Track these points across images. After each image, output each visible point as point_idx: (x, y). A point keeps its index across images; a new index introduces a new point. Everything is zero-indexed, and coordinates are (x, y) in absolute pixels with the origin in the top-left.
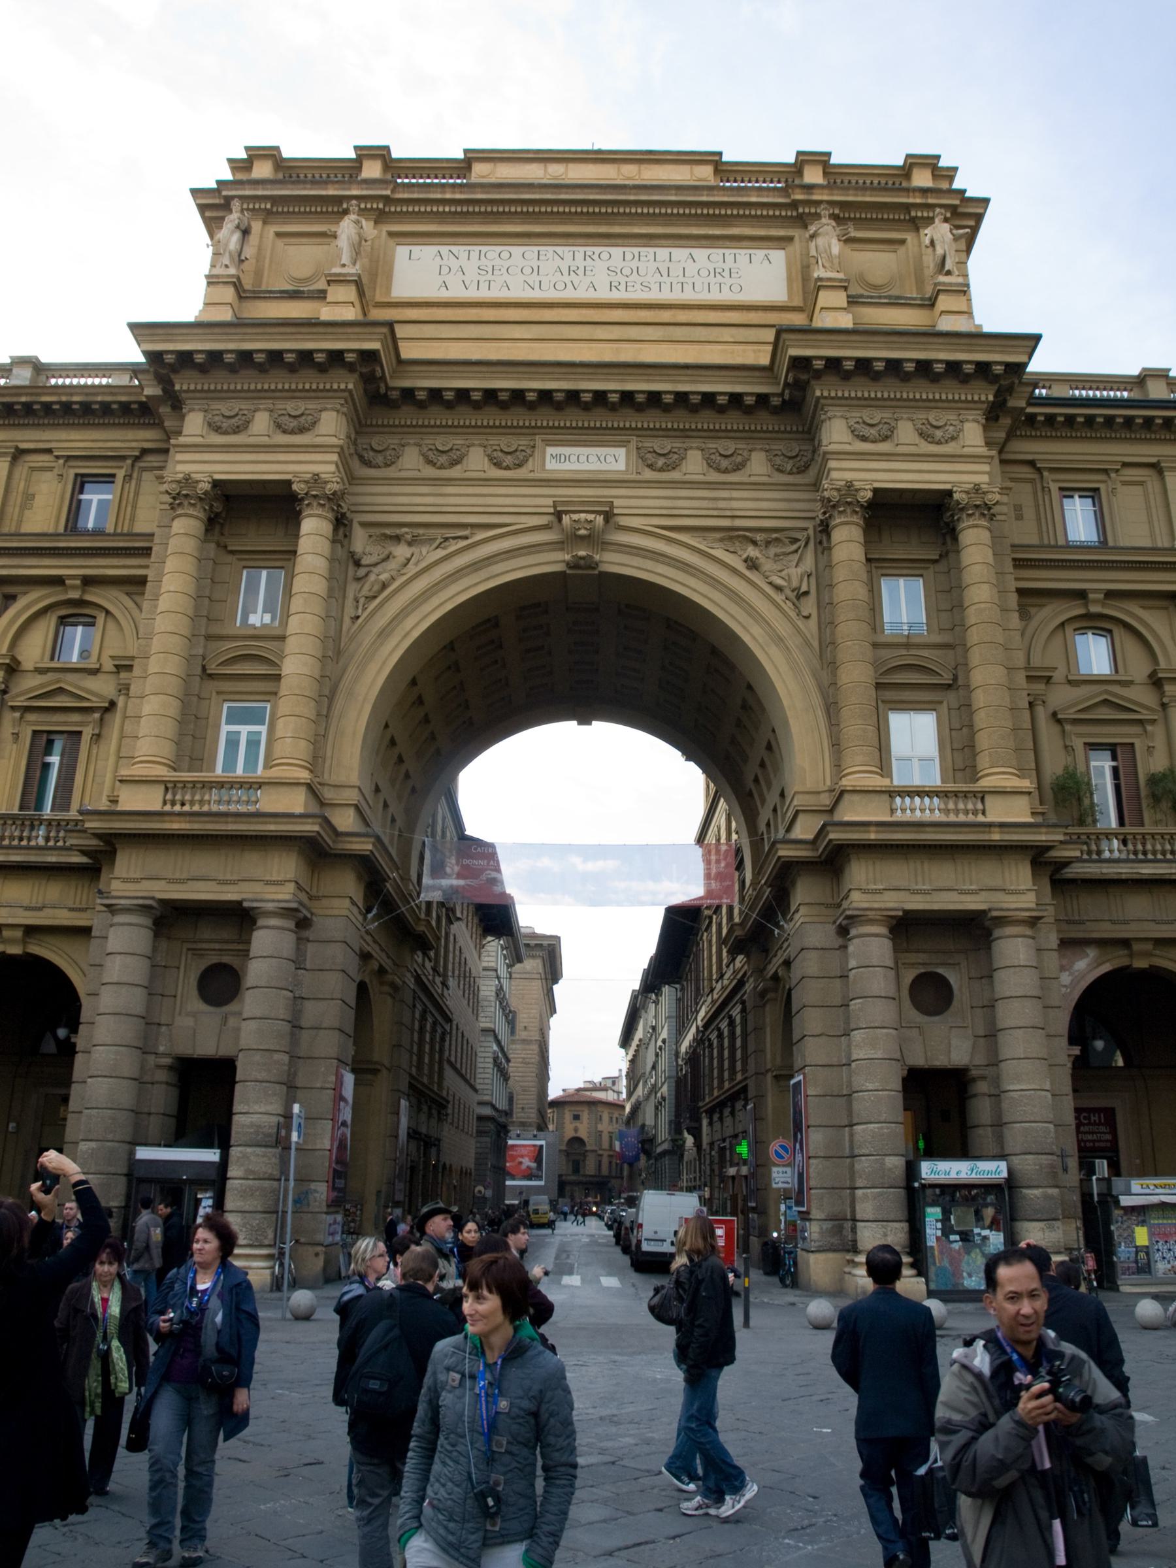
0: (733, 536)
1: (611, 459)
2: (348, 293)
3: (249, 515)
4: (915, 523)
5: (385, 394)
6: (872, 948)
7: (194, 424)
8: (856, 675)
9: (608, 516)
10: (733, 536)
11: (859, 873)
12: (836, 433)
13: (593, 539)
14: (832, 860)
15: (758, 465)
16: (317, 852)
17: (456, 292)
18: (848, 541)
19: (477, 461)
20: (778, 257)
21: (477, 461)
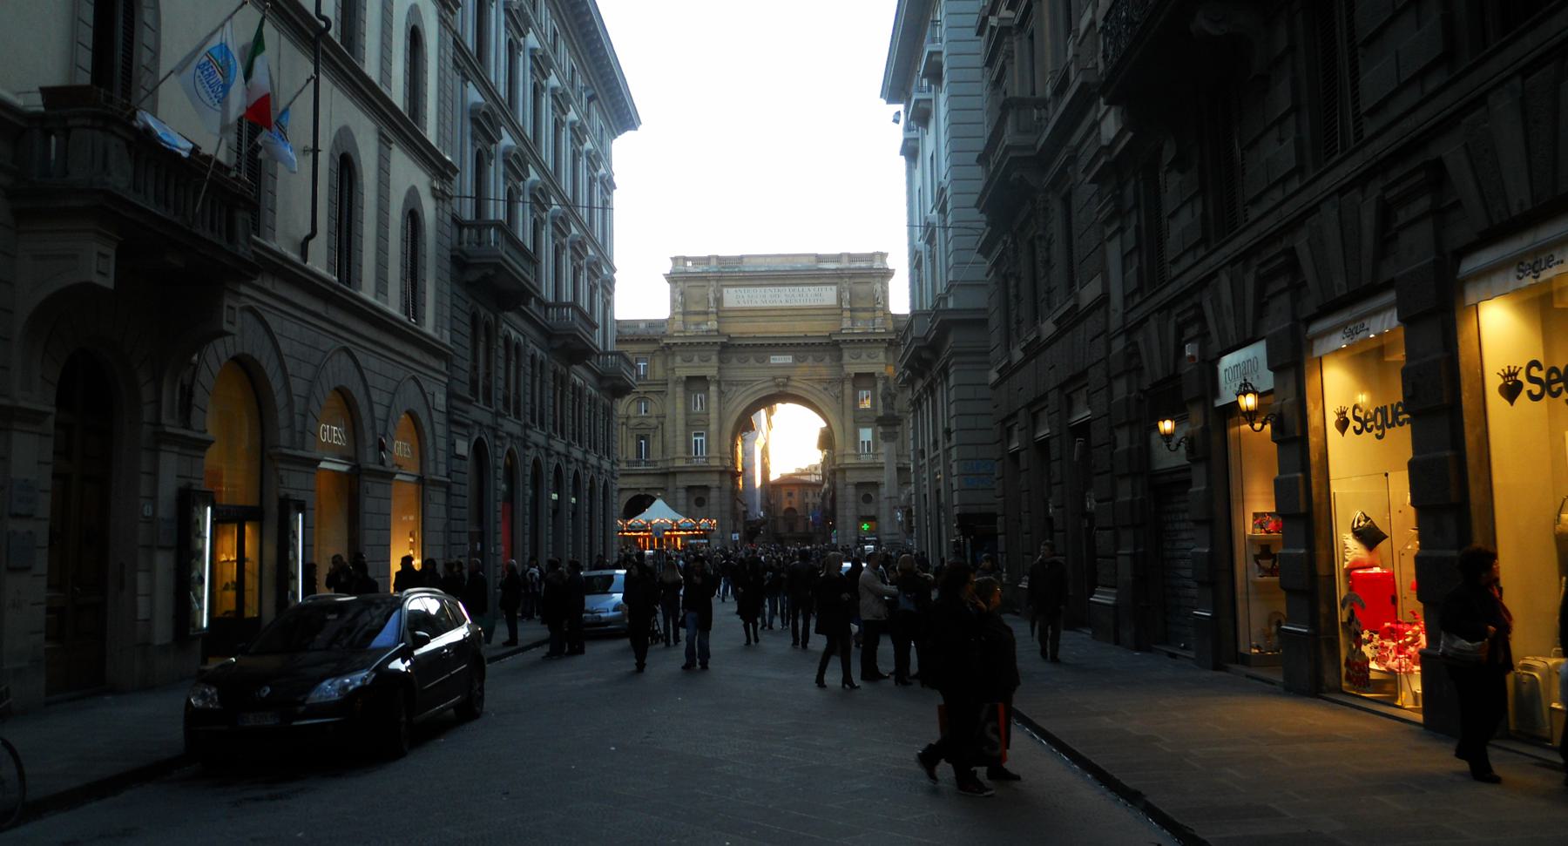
0: (820, 381)
1: (787, 359)
2: (713, 317)
3: (695, 383)
4: (863, 379)
5: (728, 348)
6: (851, 491)
7: (678, 359)
8: (849, 424)
9: (788, 378)
10: (820, 381)
11: (848, 474)
12: (846, 356)
13: (785, 385)
14: (844, 470)
15: (827, 359)
16: (721, 473)
17: (742, 305)
18: (848, 388)
19: (752, 361)
20: (834, 288)
21: (752, 361)
